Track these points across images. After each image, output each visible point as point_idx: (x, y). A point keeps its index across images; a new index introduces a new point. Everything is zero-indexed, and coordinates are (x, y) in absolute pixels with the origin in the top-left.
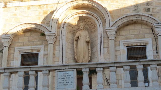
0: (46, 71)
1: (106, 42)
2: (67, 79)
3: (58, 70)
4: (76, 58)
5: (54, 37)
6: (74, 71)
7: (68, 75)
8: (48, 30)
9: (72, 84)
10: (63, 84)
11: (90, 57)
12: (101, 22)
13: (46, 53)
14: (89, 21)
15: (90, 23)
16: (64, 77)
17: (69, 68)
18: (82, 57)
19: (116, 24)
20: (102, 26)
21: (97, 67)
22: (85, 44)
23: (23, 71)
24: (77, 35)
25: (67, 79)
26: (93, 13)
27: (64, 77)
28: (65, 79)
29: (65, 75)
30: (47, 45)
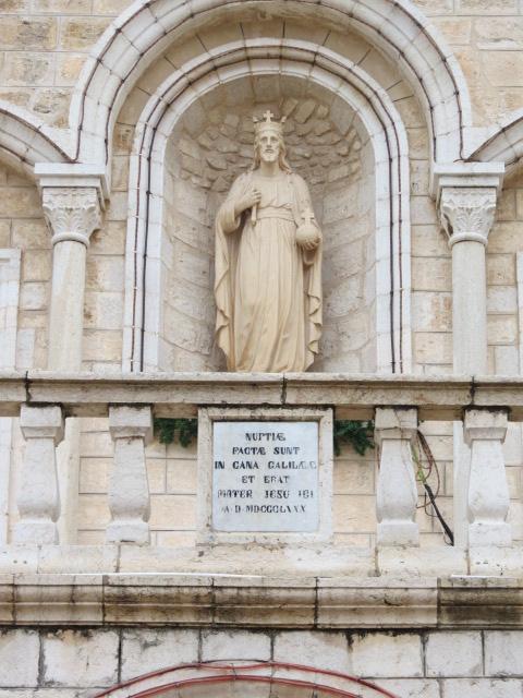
0: (133, 410)
1: (427, 253)
2: (278, 472)
3: (217, 413)
4: (226, 350)
5: (92, 197)
6: (318, 420)
8: (56, 147)
9: (308, 502)
10: (244, 502)
11: (315, 348)
12: (400, 127)
13: (34, 298)
14: (314, 112)
15: (324, 126)
16: (251, 458)
17: (291, 399)
18: (266, 340)
19: (503, 143)
20: (404, 150)
21: (471, 407)
22: (289, 260)
24: (238, 196)
25: (271, 472)
26: (349, 64)
27: (251, 458)
28: (263, 471)
29: (263, 443)
30: (46, 250)
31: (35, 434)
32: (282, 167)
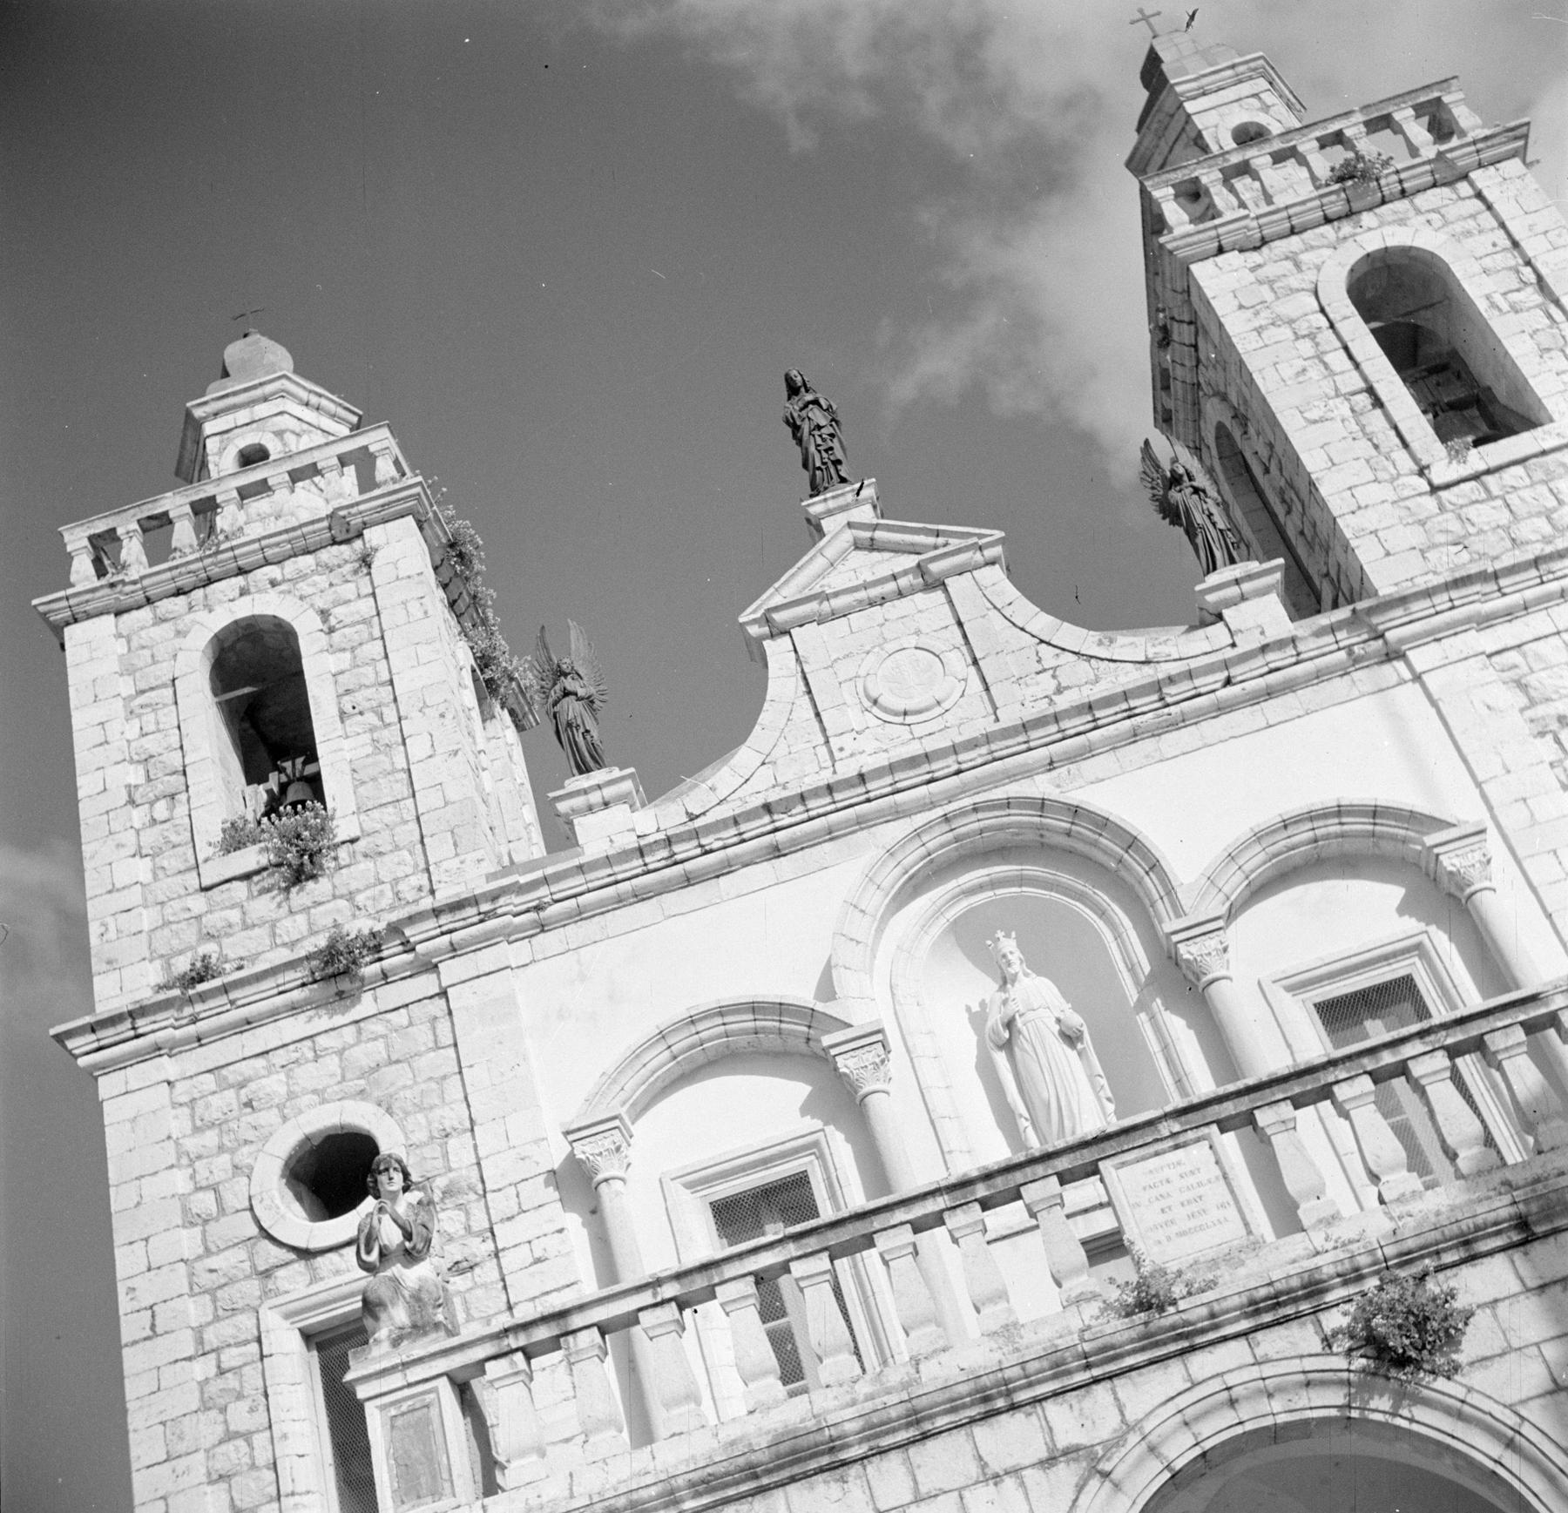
7: (1180, 1170)
10: (1174, 1229)
16: (1163, 1189)
23: (902, 1223)
29: (1167, 1173)
31: (969, 1231)
32: (1026, 975)
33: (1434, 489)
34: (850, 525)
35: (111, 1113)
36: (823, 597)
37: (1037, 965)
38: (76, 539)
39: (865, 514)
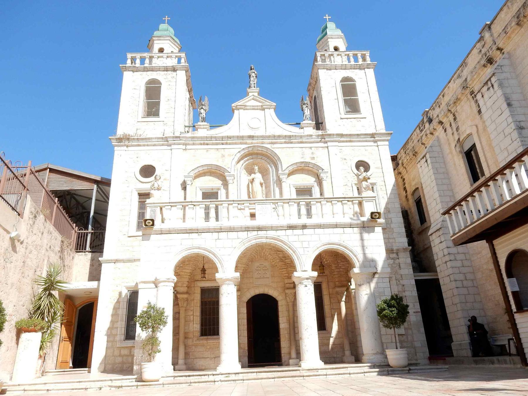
33: (341, 119)
34: (253, 95)
35: (116, 153)
36: (246, 106)
37: (260, 172)
38: (129, 56)
39: (256, 94)
